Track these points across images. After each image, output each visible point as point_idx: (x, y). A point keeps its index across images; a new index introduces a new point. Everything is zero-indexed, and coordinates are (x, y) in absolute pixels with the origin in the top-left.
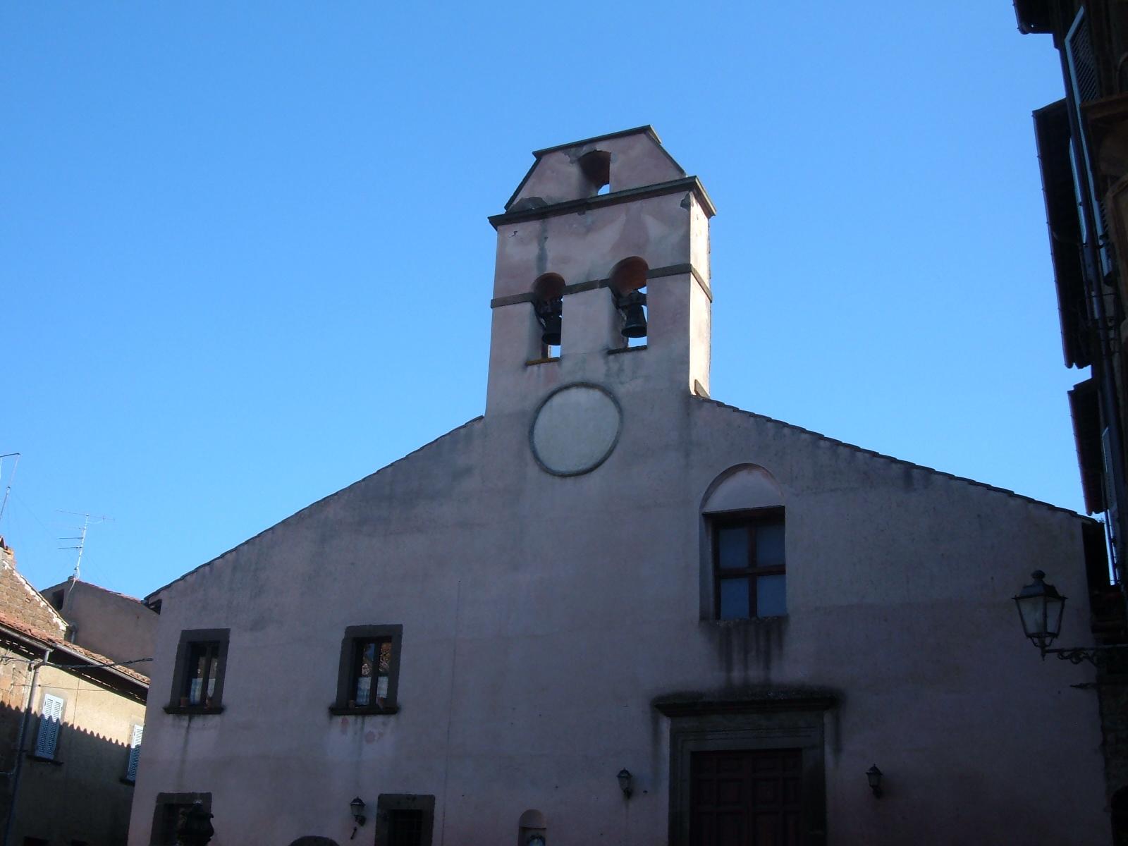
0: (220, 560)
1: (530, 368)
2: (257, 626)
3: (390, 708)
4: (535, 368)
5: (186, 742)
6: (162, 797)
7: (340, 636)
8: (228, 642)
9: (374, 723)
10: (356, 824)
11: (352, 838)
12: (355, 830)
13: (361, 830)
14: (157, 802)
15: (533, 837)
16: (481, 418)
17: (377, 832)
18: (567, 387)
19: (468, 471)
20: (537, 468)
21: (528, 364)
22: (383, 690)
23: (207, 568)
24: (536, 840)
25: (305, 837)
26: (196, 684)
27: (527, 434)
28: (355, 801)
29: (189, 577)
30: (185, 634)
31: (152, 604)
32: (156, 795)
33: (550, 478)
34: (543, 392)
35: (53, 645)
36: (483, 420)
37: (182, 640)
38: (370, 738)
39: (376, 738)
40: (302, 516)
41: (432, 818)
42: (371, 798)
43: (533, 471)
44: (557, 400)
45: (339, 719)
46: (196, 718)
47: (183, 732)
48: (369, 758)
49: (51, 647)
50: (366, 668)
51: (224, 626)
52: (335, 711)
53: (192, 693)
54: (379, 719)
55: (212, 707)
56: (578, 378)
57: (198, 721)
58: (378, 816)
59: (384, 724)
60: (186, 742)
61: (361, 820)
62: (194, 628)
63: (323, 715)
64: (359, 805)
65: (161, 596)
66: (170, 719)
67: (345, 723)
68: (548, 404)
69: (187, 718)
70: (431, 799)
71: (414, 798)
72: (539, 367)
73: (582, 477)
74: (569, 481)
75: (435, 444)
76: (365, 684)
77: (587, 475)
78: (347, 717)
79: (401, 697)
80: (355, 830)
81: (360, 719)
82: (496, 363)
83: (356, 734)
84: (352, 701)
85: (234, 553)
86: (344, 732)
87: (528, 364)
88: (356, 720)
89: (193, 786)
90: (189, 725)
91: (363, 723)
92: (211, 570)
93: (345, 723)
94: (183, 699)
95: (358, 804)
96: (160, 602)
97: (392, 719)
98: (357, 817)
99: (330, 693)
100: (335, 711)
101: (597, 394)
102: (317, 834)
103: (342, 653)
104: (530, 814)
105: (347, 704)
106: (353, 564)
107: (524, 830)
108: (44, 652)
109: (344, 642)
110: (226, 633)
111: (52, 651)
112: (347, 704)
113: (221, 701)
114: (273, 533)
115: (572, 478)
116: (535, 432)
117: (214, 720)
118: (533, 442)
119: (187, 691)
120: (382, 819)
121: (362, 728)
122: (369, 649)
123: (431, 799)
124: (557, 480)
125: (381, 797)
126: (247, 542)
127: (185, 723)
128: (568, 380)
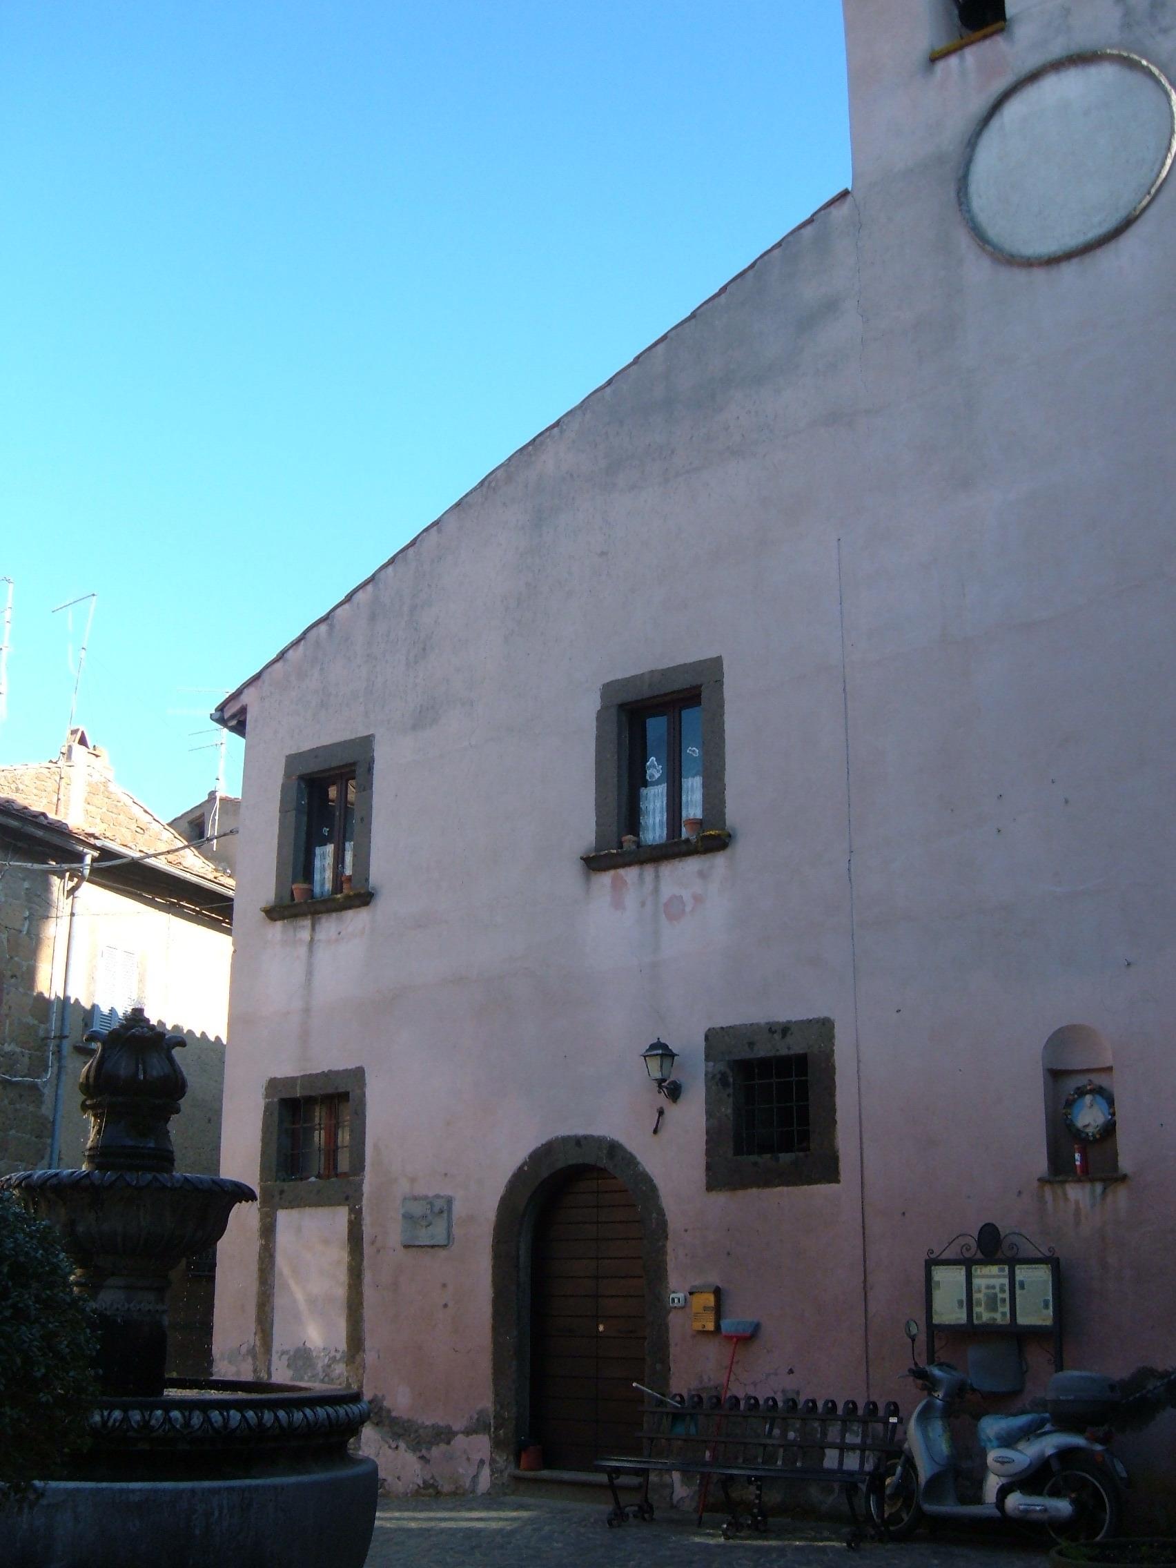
0: (346, 606)
1: (940, 65)
2: (424, 716)
3: (713, 839)
4: (953, 61)
5: (309, 973)
6: (273, 1084)
7: (590, 705)
8: (372, 760)
9: (680, 877)
10: (662, 1099)
11: (655, 1131)
12: (661, 1112)
13: (675, 1112)
14: (267, 1096)
15: (1081, 1092)
16: (845, 194)
17: (709, 1114)
18: (1033, 77)
19: (831, 306)
20: (986, 263)
21: (934, 58)
22: (693, 808)
23: (323, 628)
24: (1088, 1098)
25: (557, 1138)
26: (323, 856)
27: (953, 194)
28: (653, 1047)
29: (291, 652)
30: (292, 760)
31: (233, 717)
32: (264, 1083)
33: (1021, 276)
34: (978, 103)
35: (98, 843)
36: (849, 199)
37: (287, 775)
38: (674, 909)
39: (688, 909)
40: (493, 484)
41: (830, 1070)
42: (688, 1040)
43: (977, 271)
44: (1014, 110)
45: (606, 878)
46: (323, 920)
47: (302, 951)
48: (682, 955)
49: (94, 847)
50: (655, 768)
51: (362, 732)
52: (595, 863)
53: (317, 877)
54: (692, 865)
55: (355, 895)
56: (1057, 49)
57: (329, 926)
58: (710, 1078)
59: (702, 875)
60: (309, 973)
61: (674, 1092)
62: (306, 747)
63: (571, 872)
64: (662, 1055)
65: (245, 699)
66: (277, 930)
67: (618, 886)
68: (995, 123)
69: (307, 922)
70: (825, 1027)
71: (785, 1030)
72: (962, 59)
73: (1099, 253)
74: (1068, 271)
75: (751, 273)
76: (655, 801)
77: (1111, 247)
78: (621, 871)
79: (734, 813)
80: (661, 1112)
81: (649, 870)
82: (862, 79)
83: (643, 904)
84: (630, 837)
85: (369, 588)
86: (618, 904)
87: (934, 58)
88: (641, 876)
89: (329, 1058)
90: (312, 939)
91: (657, 877)
92: (331, 627)
93: (618, 886)
94: (299, 887)
95: (662, 1052)
96: (243, 710)
97: (719, 861)
98: (660, 1082)
99: (582, 827)
100: (595, 863)
101: (1106, 73)
102: (581, 1131)
103: (598, 738)
104: (1062, 1038)
105: (618, 847)
106: (603, 554)
107: (1055, 1075)
108: (80, 858)
109: (601, 717)
110: (366, 743)
111: (96, 854)
112: (618, 847)
113: (367, 880)
114: (439, 531)
115: (1075, 261)
116: (973, 188)
117: (357, 919)
118: (969, 211)
119: (306, 871)
120: (717, 1082)
121: (656, 891)
122: (656, 721)
123: (825, 1027)
124: (1039, 275)
125: (710, 1036)
126: (392, 561)
127: (305, 935)
128: (1033, 61)
